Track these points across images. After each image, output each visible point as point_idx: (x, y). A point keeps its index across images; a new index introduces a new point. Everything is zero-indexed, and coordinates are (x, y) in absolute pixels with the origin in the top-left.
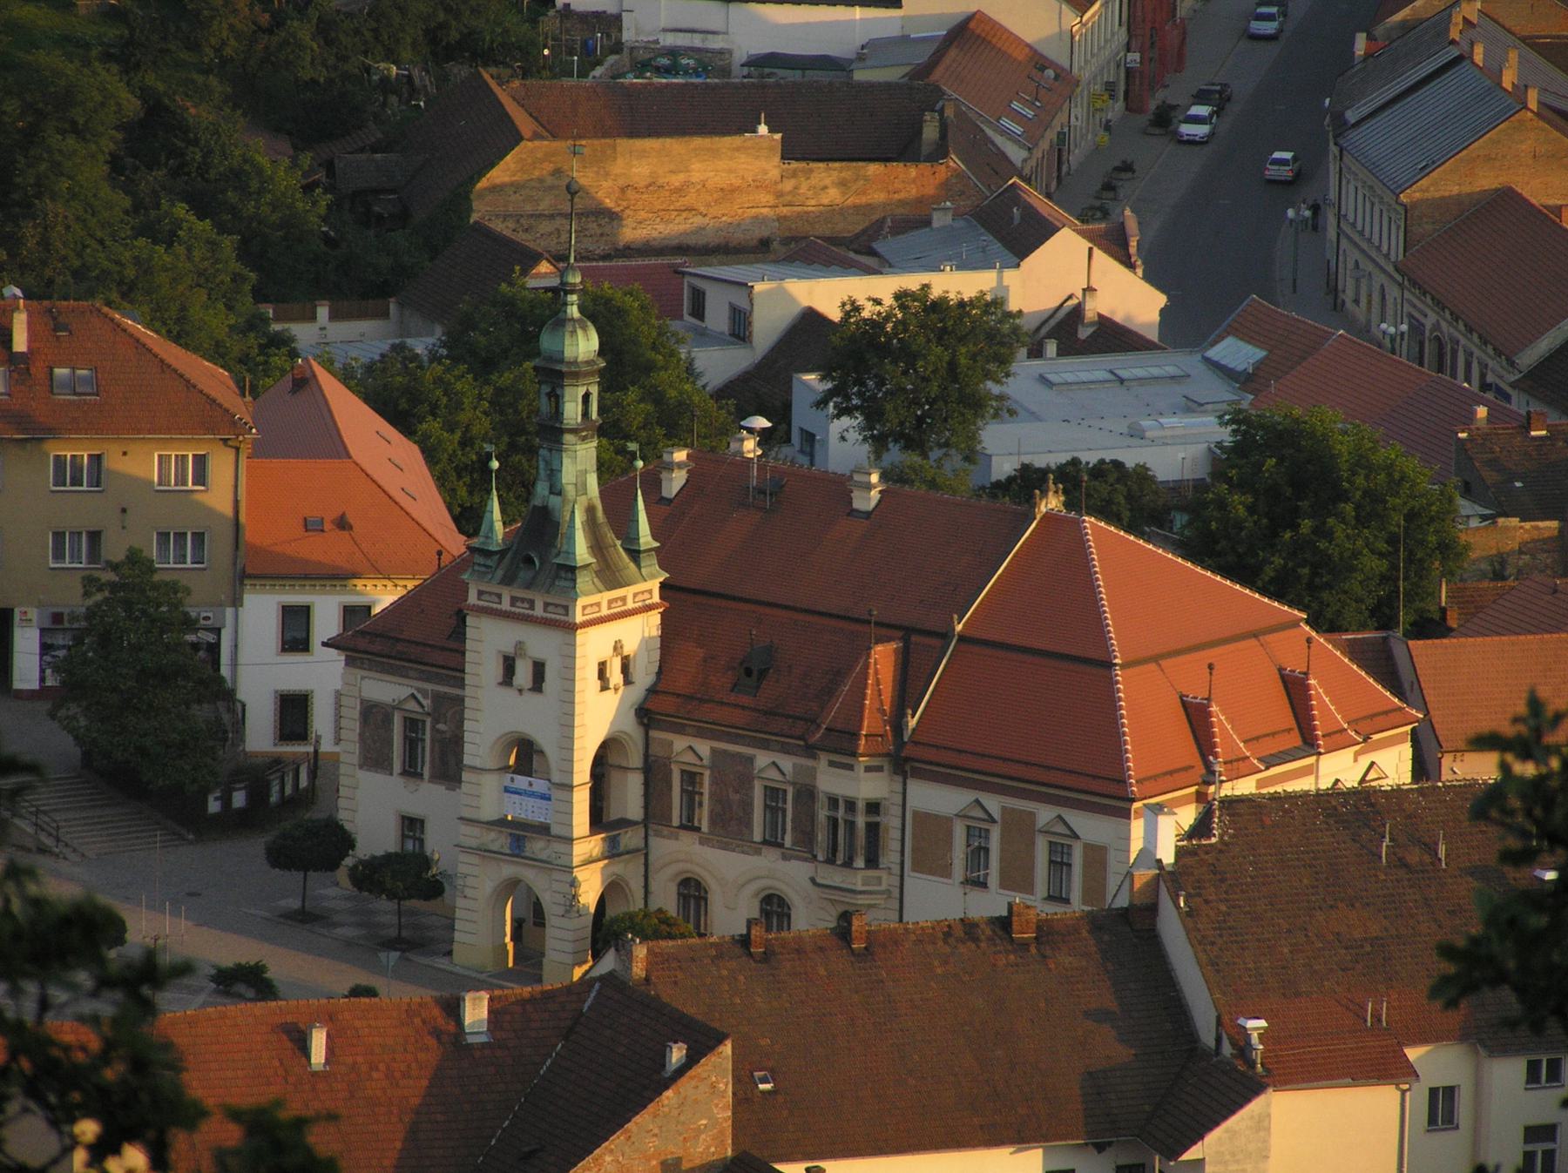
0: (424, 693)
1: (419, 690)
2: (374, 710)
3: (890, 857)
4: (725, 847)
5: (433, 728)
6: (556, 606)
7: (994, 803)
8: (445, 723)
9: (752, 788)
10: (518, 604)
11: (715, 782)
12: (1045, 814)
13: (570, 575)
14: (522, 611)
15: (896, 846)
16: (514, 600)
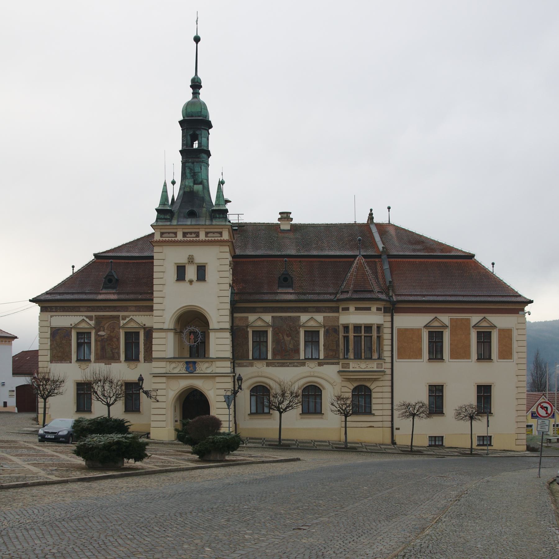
0: (90, 318)
1: (87, 317)
2: (59, 331)
3: (387, 354)
4: (283, 365)
5: (96, 334)
6: (214, 233)
8: (104, 331)
9: (298, 333)
10: (189, 235)
11: (275, 334)
13: (221, 216)
14: (191, 239)
15: (389, 348)
16: (185, 235)
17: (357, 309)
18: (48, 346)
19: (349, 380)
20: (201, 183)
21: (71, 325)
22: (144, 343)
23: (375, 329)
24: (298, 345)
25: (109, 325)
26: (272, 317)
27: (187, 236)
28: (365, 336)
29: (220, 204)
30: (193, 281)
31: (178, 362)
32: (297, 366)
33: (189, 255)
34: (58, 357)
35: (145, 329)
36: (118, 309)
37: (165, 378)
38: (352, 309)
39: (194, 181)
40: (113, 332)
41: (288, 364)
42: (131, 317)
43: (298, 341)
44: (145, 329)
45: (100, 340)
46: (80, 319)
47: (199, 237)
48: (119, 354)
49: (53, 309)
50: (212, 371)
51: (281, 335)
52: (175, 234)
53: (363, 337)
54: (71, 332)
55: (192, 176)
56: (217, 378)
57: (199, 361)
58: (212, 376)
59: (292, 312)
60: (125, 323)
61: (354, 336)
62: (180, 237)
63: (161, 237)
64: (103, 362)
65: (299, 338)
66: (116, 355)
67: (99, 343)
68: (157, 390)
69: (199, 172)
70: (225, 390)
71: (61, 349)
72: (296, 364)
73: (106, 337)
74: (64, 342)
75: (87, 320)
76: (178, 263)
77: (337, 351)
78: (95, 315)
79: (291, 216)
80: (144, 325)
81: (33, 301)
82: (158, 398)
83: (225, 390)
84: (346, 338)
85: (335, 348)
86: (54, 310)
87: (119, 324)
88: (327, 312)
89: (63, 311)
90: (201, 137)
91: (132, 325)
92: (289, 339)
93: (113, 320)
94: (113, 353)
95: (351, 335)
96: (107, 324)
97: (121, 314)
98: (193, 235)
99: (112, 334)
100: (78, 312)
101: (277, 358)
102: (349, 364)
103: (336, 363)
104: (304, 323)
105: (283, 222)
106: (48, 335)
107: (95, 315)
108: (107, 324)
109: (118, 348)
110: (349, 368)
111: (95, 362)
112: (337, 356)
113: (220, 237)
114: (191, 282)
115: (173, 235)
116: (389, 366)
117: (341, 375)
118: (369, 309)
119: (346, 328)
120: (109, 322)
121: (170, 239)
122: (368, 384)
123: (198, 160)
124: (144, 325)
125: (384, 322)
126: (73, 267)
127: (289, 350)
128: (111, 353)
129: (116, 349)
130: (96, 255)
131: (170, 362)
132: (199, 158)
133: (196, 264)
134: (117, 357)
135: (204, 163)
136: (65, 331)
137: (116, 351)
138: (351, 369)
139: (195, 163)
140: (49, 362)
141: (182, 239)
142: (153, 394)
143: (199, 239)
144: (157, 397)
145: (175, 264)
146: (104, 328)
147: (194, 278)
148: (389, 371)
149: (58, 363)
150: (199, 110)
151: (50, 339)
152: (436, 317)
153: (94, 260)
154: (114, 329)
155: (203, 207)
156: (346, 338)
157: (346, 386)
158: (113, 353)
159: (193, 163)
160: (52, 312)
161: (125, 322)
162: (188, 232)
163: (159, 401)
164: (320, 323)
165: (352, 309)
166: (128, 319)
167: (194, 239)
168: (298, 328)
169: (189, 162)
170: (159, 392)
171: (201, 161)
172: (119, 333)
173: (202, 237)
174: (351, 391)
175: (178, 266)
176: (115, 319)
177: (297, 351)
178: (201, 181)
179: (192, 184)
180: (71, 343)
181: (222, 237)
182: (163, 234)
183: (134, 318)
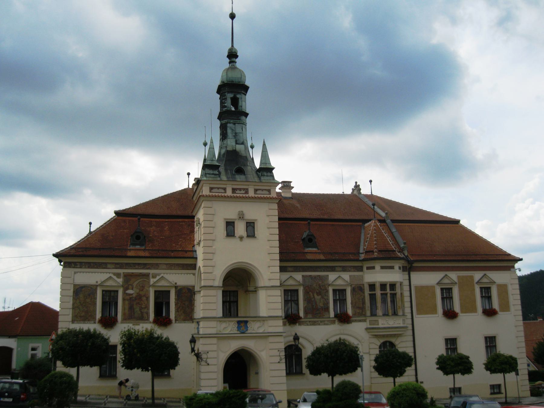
0: (118, 275)
1: (115, 274)
2: (83, 289)
4: (314, 323)
5: (124, 293)
6: (262, 190)
7: (454, 276)
8: (132, 289)
9: (327, 291)
10: (238, 192)
11: (306, 293)
12: (477, 275)
13: (269, 174)
14: (241, 195)
16: (234, 190)
17: (382, 268)
18: (70, 305)
19: (376, 336)
20: (243, 143)
21: (97, 282)
22: (175, 302)
23: (398, 286)
24: (328, 303)
25: (139, 282)
26: (303, 276)
27: (237, 192)
28: (390, 294)
29: (267, 163)
30: (243, 237)
31: (229, 321)
32: (327, 324)
33: (239, 211)
34: (80, 317)
35: (176, 287)
36: (148, 267)
37: (216, 339)
38: (378, 267)
39: (236, 141)
40: (142, 290)
41: (319, 322)
42: (162, 275)
43: (328, 299)
44: (176, 287)
45: (128, 299)
46: (107, 276)
47: (248, 194)
48: (148, 314)
49: (77, 265)
50: (264, 331)
51: (311, 294)
52: (225, 189)
53: (389, 295)
54: (97, 289)
55: (234, 136)
56: (270, 338)
57: (251, 321)
58: (265, 336)
59: (312, 271)
60: (155, 281)
61: (381, 294)
62: (229, 193)
63: (210, 192)
64: (131, 323)
65: (328, 296)
66: (145, 315)
67: (127, 302)
68: (208, 353)
69: (240, 133)
70: (279, 351)
71: (84, 308)
72: (326, 322)
73: (134, 295)
74: (88, 300)
75: (115, 277)
76: (227, 219)
77: (363, 308)
78: (123, 273)
79: (292, 185)
80: (176, 283)
81: (55, 255)
82: (209, 361)
83: (279, 351)
84: (373, 297)
85: (361, 306)
86: (78, 266)
87: (149, 282)
88: (352, 271)
89: (89, 268)
90: (242, 101)
91: (163, 283)
92: (320, 297)
93: (143, 278)
94: (142, 312)
95: (378, 292)
96: (137, 282)
97: (151, 272)
98: (243, 192)
99: (141, 293)
100: (104, 268)
101: (308, 317)
102: (378, 321)
103: (363, 320)
104: (333, 282)
105: (285, 190)
106: (71, 293)
107: (123, 273)
108: (137, 282)
109: (147, 307)
110: (378, 325)
111: (122, 323)
112: (364, 313)
113: (268, 194)
114: (241, 238)
115: (223, 191)
116: (410, 321)
117: (368, 332)
118: (392, 268)
119: (372, 286)
120: (138, 280)
121: (221, 194)
122: (393, 340)
123: (239, 122)
124: (176, 283)
125: (404, 280)
126: (90, 224)
127: (320, 308)
128: (139, 312)
129: (145, 308)
130: (116, 213)
131: (220, 321)
132: (240, 120)
133: (246, 220)
134: (146, 316)
135: (244, 125)
136: (89, 288)
137: (146, 310)
138: (380, 326)
139: (236, 124)
140: (71, 323)
141: (232, 195)
142: (204, 356)
143: (249, 196)
144: (208, 360)
145: (225, 219)
146: (133, 286)
147: (244, 234)
148: (410, 327)
149: (81, 323)
150: (239, 76)
151: (73, 298)
152: (446, 275)
153: (115, 217)
154: (143, 287)
155: (247, 166)
156: (373, 297)
157: (373, 343)
158: (142, 312)
159: (234, 124)
160: (77, 268)
161: (155, 280)
162: (238, 189)
163: (210, 364)
164: (347, 282)
165: (378, 267)
166: (158, 278)
167: (244, 195)
168: (327, 286)
169: (230, 123)
170: (211, 355)
171: (242, 123)
172: (148, 291)
173: (251, 193)
174: (378, 347)
175: (227, 222)
176: (145, 277)
177: (327, 309)
178: (243, 142)
179: (234, 144)
180: (96, 301)
181: (270, 194)
182: (212, 189)
183: (165, 276)
